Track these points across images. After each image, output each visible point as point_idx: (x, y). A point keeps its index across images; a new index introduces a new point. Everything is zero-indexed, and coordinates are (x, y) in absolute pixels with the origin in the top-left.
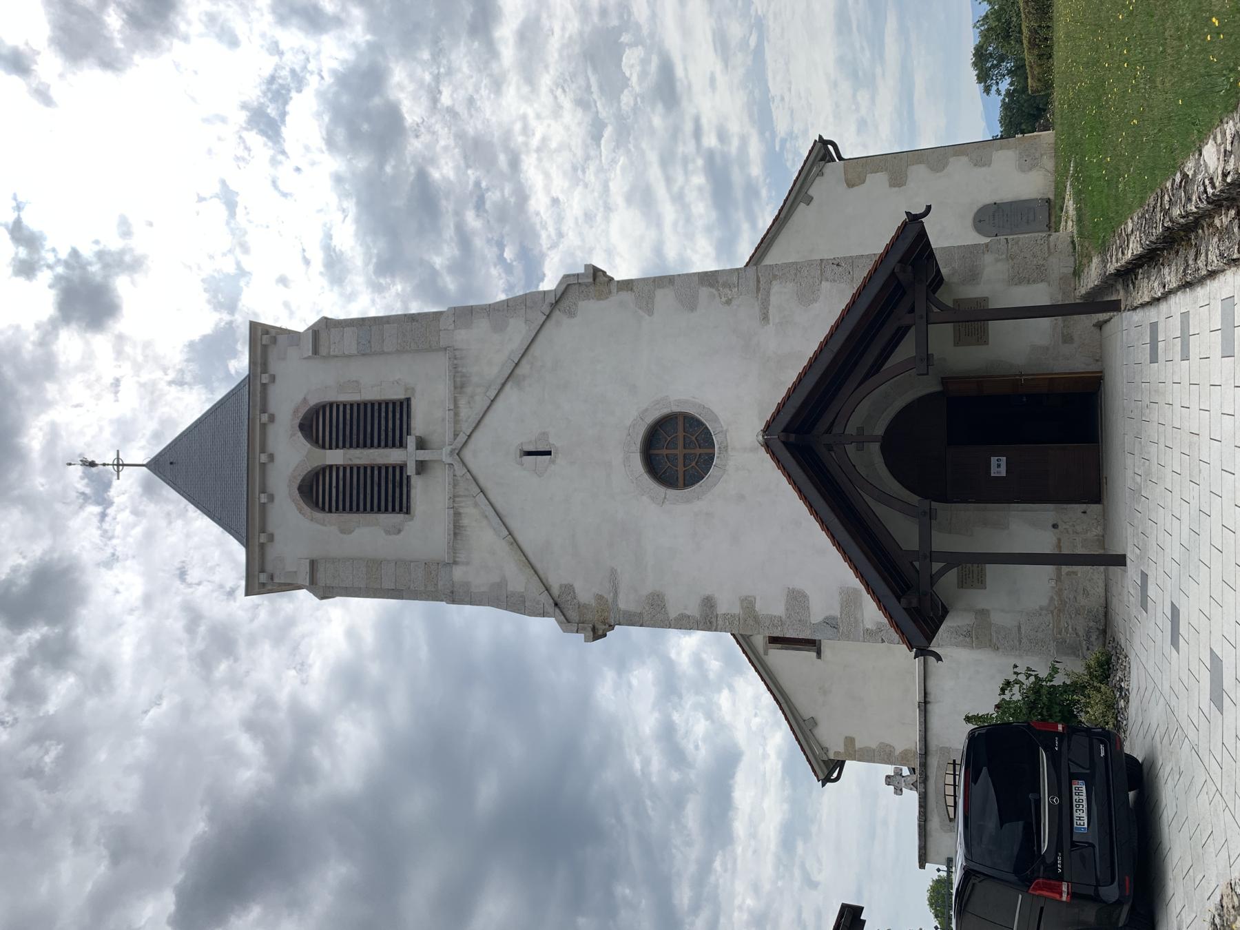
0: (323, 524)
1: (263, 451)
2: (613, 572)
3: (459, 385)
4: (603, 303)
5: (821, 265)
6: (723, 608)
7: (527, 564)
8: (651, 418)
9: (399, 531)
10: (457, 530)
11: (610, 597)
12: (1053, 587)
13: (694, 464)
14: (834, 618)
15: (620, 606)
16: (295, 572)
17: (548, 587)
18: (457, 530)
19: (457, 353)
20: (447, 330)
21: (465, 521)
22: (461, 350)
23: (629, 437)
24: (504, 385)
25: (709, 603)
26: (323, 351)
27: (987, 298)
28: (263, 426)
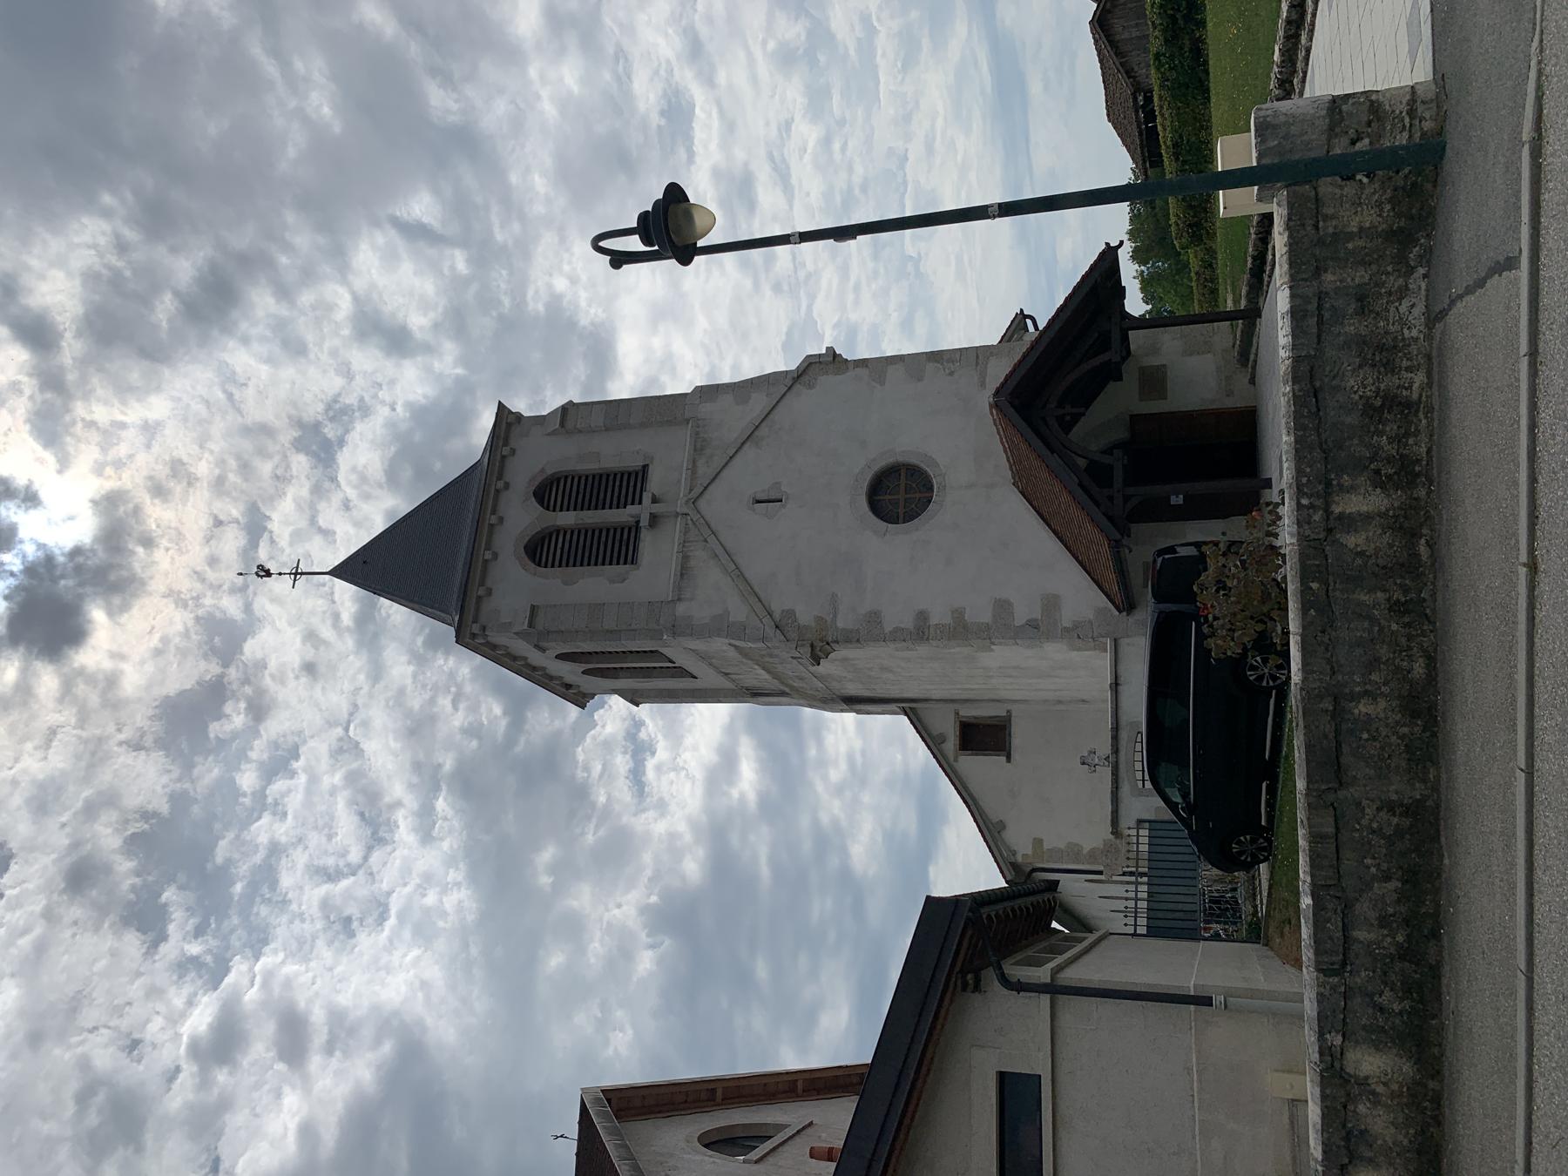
1: (494, 512)
2: (834, 596)
3: (699, 447)
6: (934, 621)
8: (877, 467)
10: (684, 572)
14: (1036, 620)
16: (510, 623)
18: (684, 572)
21: (692, 563)
22: (704, 419)
24: (743, 444)
25: (922, 616)
26: (569, 424)
28: (497, 491)
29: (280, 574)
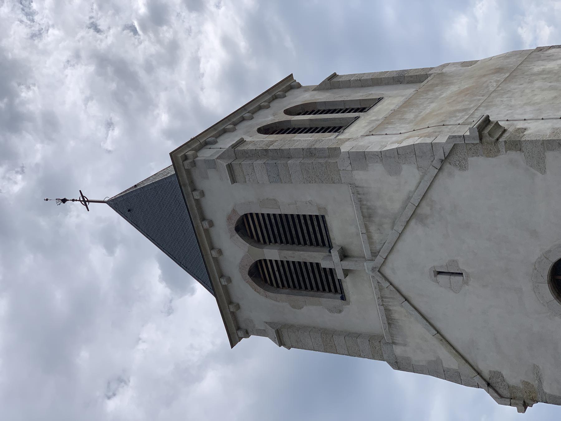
0: (276, 301)
2: (535, 367)
4: (493, 160)
9: (340, 311)
11: (536, 383)
15: (545, 390)
17: (479, 371)
20: (346, 170)
21: (396, 316)
22: (363, 187)
23: (536, 271)
24: (408, 222)
29: (73, 200)
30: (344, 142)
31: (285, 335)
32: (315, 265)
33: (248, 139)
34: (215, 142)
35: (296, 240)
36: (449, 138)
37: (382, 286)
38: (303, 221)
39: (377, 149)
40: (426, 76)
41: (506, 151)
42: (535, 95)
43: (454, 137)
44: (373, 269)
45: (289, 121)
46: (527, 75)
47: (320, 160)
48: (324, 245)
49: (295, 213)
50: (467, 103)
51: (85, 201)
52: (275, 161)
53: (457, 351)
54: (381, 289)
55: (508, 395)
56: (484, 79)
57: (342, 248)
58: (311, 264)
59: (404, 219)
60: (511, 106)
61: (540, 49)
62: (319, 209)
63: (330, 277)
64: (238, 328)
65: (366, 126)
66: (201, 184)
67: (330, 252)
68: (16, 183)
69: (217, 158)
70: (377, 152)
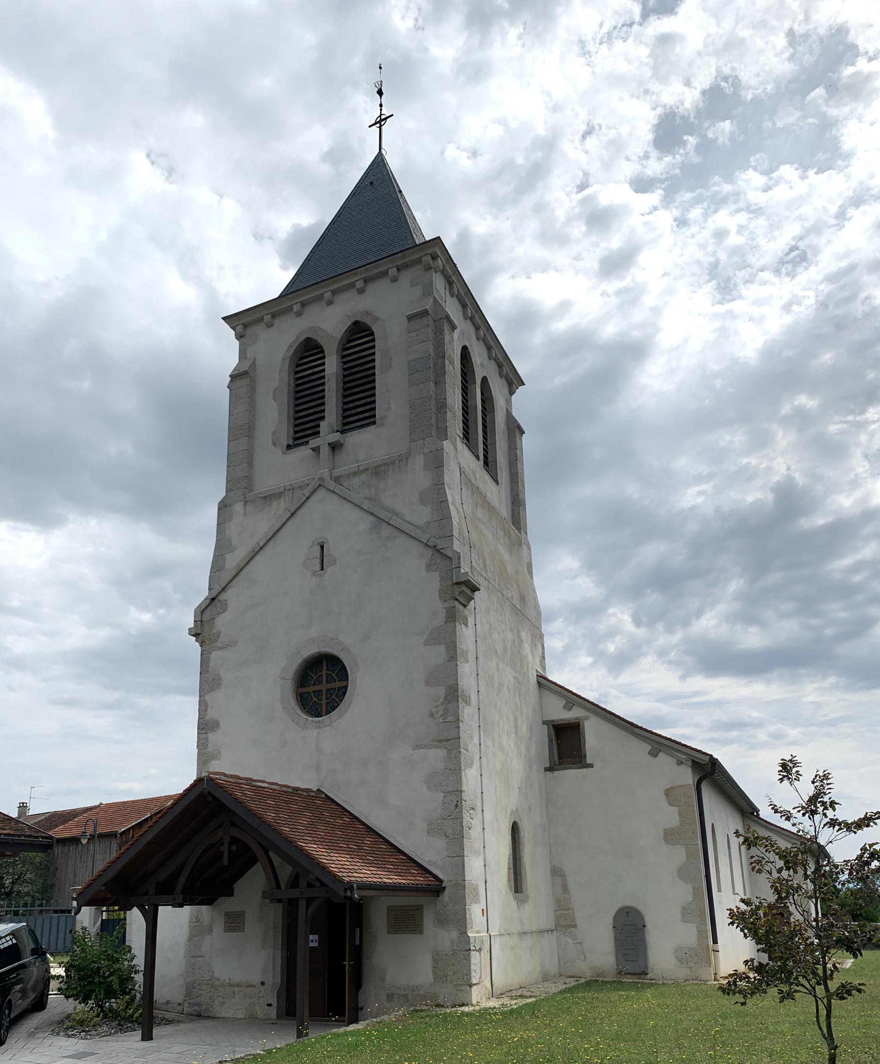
0: (280, 371)
2: (234, 643)
4: (436, 596)
5: (457, 791)
6: (211, 736)
7: (240, 568)
9: (274, 444)
11: (218, 644)
12: (225, 981)
13: (315, 699)
15: (213, 653)
17: (225, 590)
19: (404, 462)
21: (274, 504)
24: (372, 514)
27: (422, 934)
30: (453, 445)
31: (244, 382)
32: (322, 415)
33: (456, 334)
34: (452, 295)
35: (347, 393)
36: (458, 552)
37: (305, 488)
38: (368, 400)
39: (446, 479)
40: (519, 529)
41: (444, 608)
42: (499, 634)
43: (459, 558)
44: (322, 479)
45: (475, 383)
46: (518, 625)
47: (434, 417)
48: (344, 424)
49: (377, 392)
50: (492, 569)
51: (380, 122)
52: (432, 367)
53: (244, 567)
54: (301, 488)
55: (205, 619)
56: (515, 586)
57: (342, 444)
58: (323, 411)
59: (375, 510)
60: (488, 611)
61: (541, 636)
62: (382, 418)
63: (310, 432)
64: (245, 326)
65: (469, 467)
66: (406, 276)
67: (337, 431)
68: (403, 18)
69: (434, 297)
70: (443, 479)
